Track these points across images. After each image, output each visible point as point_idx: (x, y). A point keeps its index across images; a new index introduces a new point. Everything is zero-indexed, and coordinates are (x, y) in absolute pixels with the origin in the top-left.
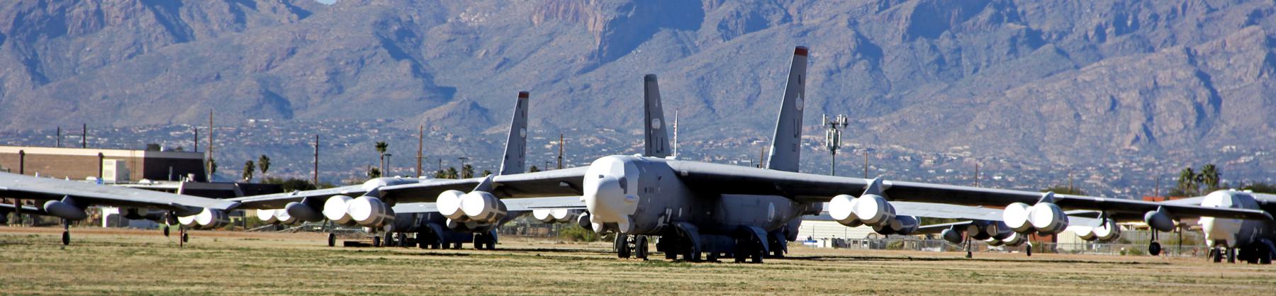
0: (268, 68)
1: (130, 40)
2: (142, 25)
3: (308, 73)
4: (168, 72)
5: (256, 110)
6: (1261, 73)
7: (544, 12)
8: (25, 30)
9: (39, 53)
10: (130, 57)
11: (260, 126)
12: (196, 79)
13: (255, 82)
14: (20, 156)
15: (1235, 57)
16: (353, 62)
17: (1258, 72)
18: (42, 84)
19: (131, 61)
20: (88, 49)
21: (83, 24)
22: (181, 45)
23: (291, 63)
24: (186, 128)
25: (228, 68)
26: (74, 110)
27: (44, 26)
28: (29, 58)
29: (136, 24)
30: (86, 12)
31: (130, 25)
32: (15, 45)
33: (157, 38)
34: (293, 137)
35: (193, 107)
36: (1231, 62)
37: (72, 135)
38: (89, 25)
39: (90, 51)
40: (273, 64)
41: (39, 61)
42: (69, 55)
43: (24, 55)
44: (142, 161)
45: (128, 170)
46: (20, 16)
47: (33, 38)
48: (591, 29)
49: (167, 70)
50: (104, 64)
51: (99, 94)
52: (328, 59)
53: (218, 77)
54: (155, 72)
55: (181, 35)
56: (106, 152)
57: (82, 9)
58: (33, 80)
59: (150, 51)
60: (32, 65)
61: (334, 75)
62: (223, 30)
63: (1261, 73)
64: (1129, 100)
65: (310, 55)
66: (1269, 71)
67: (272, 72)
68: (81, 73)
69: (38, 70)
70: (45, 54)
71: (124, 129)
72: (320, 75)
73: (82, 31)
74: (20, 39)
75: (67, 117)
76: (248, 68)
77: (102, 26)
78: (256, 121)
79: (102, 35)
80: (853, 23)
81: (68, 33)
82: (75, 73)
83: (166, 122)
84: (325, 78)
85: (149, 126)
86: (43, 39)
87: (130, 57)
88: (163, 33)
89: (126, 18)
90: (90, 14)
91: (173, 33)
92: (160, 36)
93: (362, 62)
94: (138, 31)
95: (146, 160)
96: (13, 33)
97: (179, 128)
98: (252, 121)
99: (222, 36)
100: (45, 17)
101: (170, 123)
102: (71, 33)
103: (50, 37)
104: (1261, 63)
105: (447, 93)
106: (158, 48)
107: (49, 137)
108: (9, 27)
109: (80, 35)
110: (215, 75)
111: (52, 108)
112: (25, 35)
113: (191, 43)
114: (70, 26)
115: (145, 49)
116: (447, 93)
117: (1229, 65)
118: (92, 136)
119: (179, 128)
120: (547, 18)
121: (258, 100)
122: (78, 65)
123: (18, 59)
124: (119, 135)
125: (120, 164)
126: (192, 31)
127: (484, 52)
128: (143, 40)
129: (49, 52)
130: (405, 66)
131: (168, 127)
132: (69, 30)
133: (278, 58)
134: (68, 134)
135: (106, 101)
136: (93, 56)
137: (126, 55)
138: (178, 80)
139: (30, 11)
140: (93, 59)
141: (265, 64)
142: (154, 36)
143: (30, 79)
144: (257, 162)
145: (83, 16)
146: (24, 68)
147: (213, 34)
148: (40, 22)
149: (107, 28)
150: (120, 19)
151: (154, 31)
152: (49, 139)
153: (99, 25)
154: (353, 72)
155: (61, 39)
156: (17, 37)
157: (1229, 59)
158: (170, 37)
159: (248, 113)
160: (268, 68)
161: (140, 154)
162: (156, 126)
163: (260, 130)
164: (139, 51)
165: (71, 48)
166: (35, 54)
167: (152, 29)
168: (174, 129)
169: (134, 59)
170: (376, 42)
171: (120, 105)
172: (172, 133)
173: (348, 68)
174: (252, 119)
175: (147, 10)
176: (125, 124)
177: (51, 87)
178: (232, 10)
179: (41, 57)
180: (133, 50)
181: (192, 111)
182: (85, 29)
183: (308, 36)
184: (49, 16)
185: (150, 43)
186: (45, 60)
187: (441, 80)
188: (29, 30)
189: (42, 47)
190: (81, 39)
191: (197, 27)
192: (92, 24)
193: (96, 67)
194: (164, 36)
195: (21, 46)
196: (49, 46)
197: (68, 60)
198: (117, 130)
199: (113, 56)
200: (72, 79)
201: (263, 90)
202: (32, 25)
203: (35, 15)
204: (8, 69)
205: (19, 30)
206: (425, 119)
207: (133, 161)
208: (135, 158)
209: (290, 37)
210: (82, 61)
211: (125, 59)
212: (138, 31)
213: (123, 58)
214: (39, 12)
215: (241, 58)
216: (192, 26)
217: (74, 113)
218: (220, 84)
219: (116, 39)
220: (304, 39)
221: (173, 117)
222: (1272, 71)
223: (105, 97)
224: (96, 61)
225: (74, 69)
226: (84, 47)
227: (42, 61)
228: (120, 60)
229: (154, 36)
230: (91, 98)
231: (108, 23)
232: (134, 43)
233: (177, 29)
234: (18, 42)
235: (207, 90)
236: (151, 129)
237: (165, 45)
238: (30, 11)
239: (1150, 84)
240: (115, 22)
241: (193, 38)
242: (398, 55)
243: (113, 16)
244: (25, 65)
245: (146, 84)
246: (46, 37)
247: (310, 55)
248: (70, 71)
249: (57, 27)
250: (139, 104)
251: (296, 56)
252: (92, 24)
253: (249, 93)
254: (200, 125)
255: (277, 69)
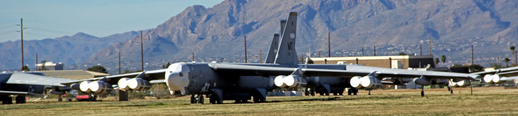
0: (428, 18)
1: (368, 9)
2: (373, 3)
3: (445, 19)
4: (385, 23)
5: (424, 37)
8: (324, 9)
9: (331, 18)
10: (369, 17)
11: (425, 43)
12: (397, 24)
13: (422, 25)
14: (356, 61)
16: (464, 13)
18: (333, 31)
19: (369, 19)
20: (351, 15)
21: (349, 5)
22: (390, 11)
23: (438, 15)
24: (394, 46)
25: (411, 19)
26: (347, 40)
27: (332, 6)
28: (327, 20)
31: (368, 4)
32: (321, 15)
33: (380, 9)
34: (440, 47)
35: (396, 37)
37: (346, 52)
38: (351, 4)
39: (352, 15)
40: (430, 16)
41: (331, 21)
42: (343, 18)
43: (325, 19)
44: (408, 60)
45: (402, 64)
46: (322, 3)
47: (328, 11)
49: (385, 22)
50: (358, 20)
51: (357, 34)
52: (453, 13)
53: (407, 23)
54: (379, 23)
55: (390, 6)
56: (392, 57)
58: (329, 29)
59: (377, 14)
60: (329, 23)
61: (457, 20)
62: (408, 3)
65: (446, 12)
67: (430, 20)
68: (349, 25)
69: (331, 25)
70: (333, 18)
71: (368, 48)
73: (348, 7)
74: (323, 12)
75: (344, 44)
76: (419, 19)
77: (357, 5)
78: (424, 41)
79: (357, 9)
81: (343, 8)
82: (346, 25)
83: (385, 44)
84: (453, 21)
85: (379, 46)
86: (332, 12)
87: (369, 17)
88: (382, 6)
91: (387, 6)
92: (381, 8)
93: (468, 13)
94: (372, 6)
95: (410, 60)
96: (320, 10)
97: (392, 46)
98: (422, 41)
99: (408, 6)
100: (333, 2)
101: (387, 44)
102: (344, 8)
103: (336, 10)
105: (507, 25)
106: (381, 12)
107: (337, 53)
108: (318, 8)
109: (348, 9)
110: (405, 23)
111: (338, 41)
112: (325, 10)
113: (395, 10)
114: (343, 5)
115: (375, 13)
116: (507, 25)
118: (355, 51)
119: (392, 46)
121: (424, 32)
122: (347, 22)
123: (323, 20)
124: (366, 50)
125: (399, 62)
126: (394, 4)
128: (374, 10)
129: (335, 17)
130: (487, 14)
131: (387, 46)
132: (343, 7)
133: (432, 14)
134: (345, 51)
135: (360, 36)
136: (354, 18)
137: (367, 16)
138: (390, 25)
140: (354, 19)
141: (426, 17)
142: (378, 8)
143: (328, 29)
144: (440, 59)
146: (325, 24)
147: (403, 5)
148: (331, 5)
149: (359, 6)
151: (379, 5)
152: (337, 54)
153: (355, 4)
154: (465, 18)
155: (340, 11)
156: (322, 12)
158: (385, 8)
159: (420, 38)
160: (428, 18)
161: (407, 57)
162: (381, 46)
163: (426, 45)
164: (373, 14)
165: (344, 15)
166: (329, 18)
167: (377, 5)
168: (389, 47)
169: (371, 18)
170: (474, 4)
171: (366, 38)
172: (388, 49)
173: (463, 16)
174: (422, 40)
176: (368, 46)
177: (336, 32)
179: (332, 20)
180: (370, 14)
181: (396, 38)
182: (350, 7)
183: (444, 3)
184: (334, 2)
185: (377, 11)
186: (334, 21)
187: (503, 19)
188: (327, 8)
189: (332, 15)
190: (348, 11)
191: (397, 3)
192: (352, 5)
193: (355, 22)
194: (383, 7)
195: (323, 15)
196: (335, 15)
197: (343, 20)
198: (365, 48)
199: (362, 17)
200: (345, 28)
201: (426, 28)
202: (327, 6)
203: (329, 2)
204: (318, 25)
205: (322, 8)
206: (497, 36)
207: (404, 60)
208: (405, 59)
209: (437, 5)
210: (349, 20)
211: (367, 18)
212: (372, 6)
213: (366, 18)
215: (416, 15)
216: (394, 2)
217: (347, 42)
218: (408, 27)
219: (363, 10)
220: (443, 5)
221: (388, 41)
223: (359, 35)
224: (355, 20)
225: (346, 24)
226: (349, 14)
227: (332, 21)
228: (365, 19)
229: (378, 8)
230: (354, 35)
231: (359, 3)
232: (370, 11)
233: (388, 4)
234: (322, 14)
235: (402, 29)
236: (379, 47)
237: (384, 11)
240: (362, 3)
241: (395, 8)
242: (484, 9)
244: (325, 23)
245: (376, 28)
246: (333, 11)
247: (446, 12)
248: (344, 24)
249: (338, 6)
250: (374, 37)
251: (439, 12)
252: (352, 5)
253: (420, 29)
254: (400, 44)
255: (432, 19)
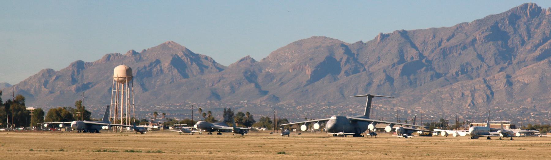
16: (237, 84)
18: (146, 91)
21: (157, 74)
29: (172, 73)
30: (157, 70)
33: (178, 77)
40: (214, 84)
57: (156, 69)
58: (143, 90)
61: (232, 88)
67: (213, 87)
72: (228, 88)
79: (162, 77)
89: (169, 71)
90: (159, 70)
93: (240, 83)
128: (174, 78)
133: (215, 83)
139: (141, 70)
145: (157, 71)
146: (140, 86)
150: (167, 72)
154: (237, 87)
164: (173, 81)
170: (244, 78)
173: (236, 86)
175: (175, 69)
178: (199, 69)
180: (171, 81)
199: (165, 83)
214: (144, 70)
238: (141, 70)
242: (251, 81)
243: (165, 71)
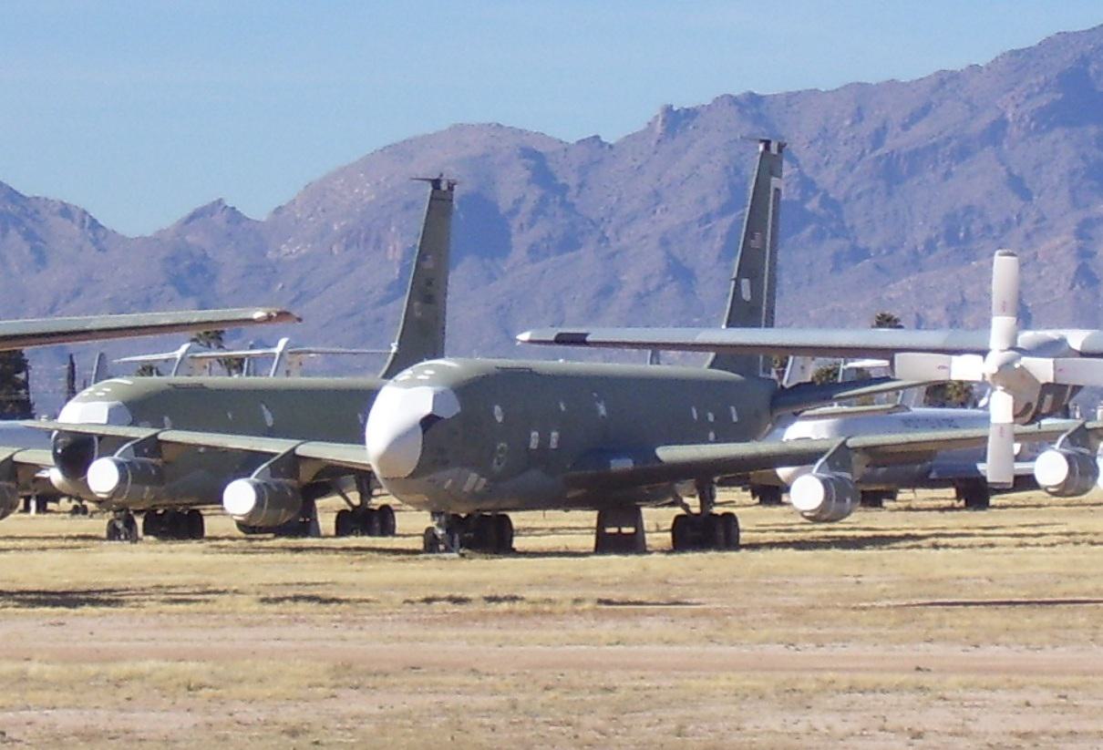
6: (1073, 286)
7: (344, 240)
15: (1047, 268)
17: (1069, 284)
36: (1043, 273)
48: (390, 257)
63: (1073, 286)
64: (935, 318)
66: (1080, 283)
80: (664, 243)
104: (1071, 277)
117: (1040, 278)
120: (347, 247)
127: (280, 285)
157: (1039, 272)
222: (1084, 283)
239: (958, 300)
